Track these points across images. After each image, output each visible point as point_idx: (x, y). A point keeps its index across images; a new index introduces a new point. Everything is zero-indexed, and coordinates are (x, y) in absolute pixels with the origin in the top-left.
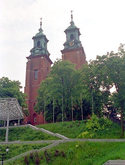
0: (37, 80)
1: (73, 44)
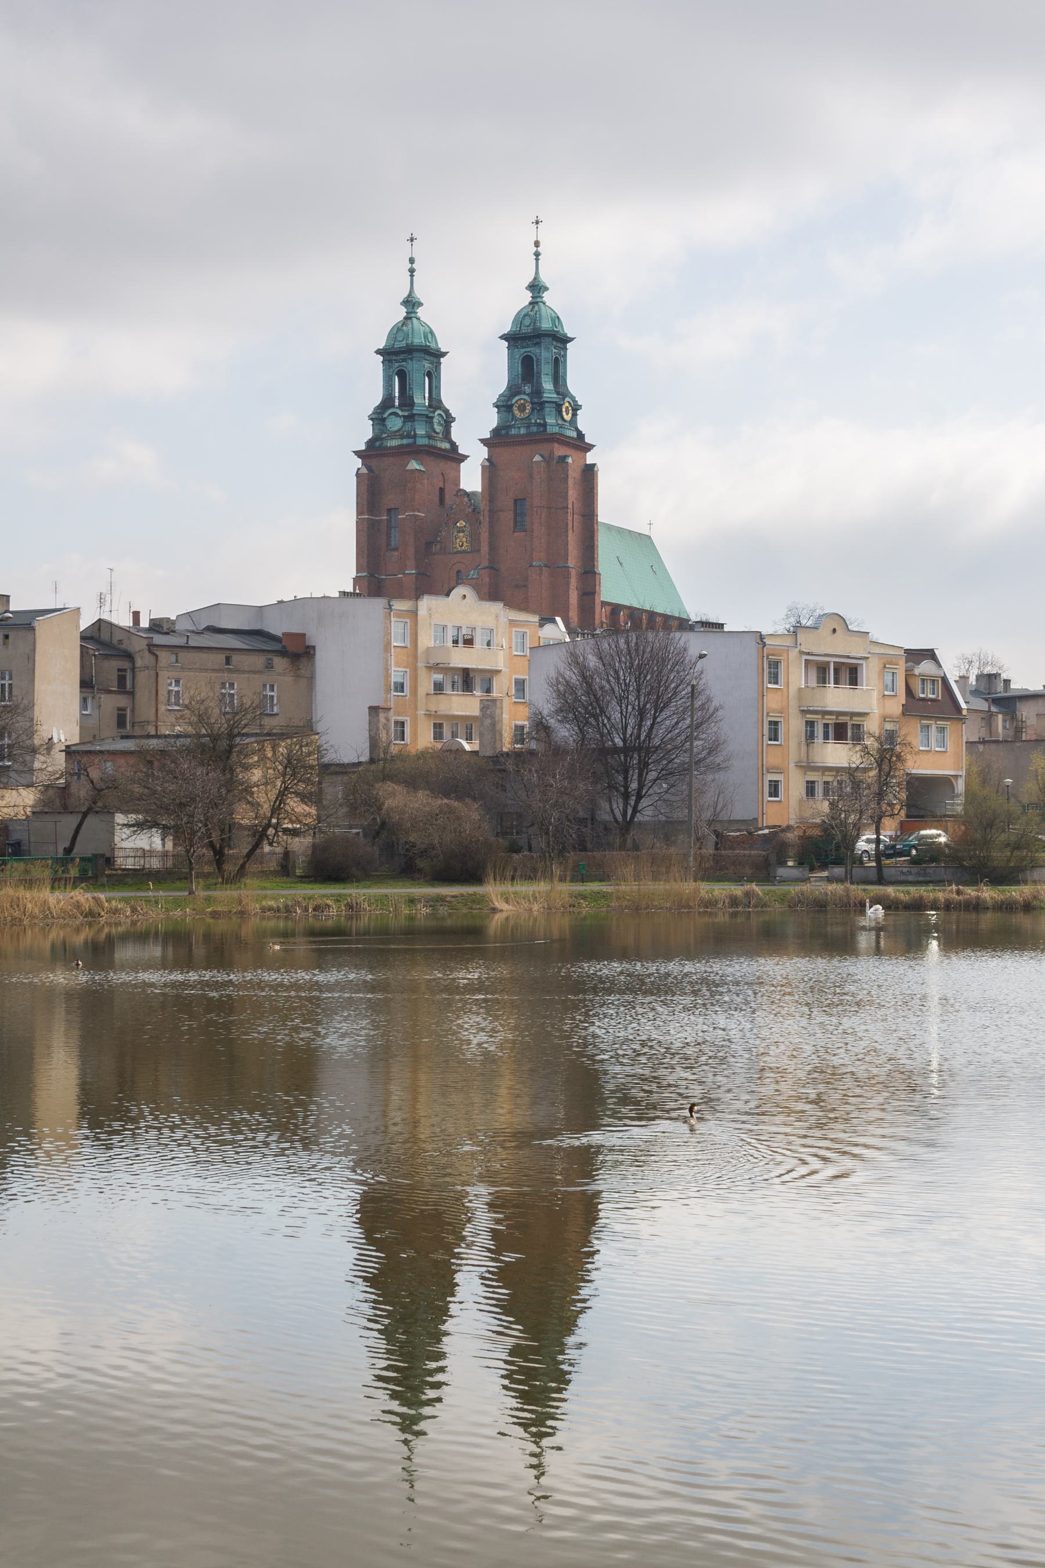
0: (396, 553)
1: (529, 407)
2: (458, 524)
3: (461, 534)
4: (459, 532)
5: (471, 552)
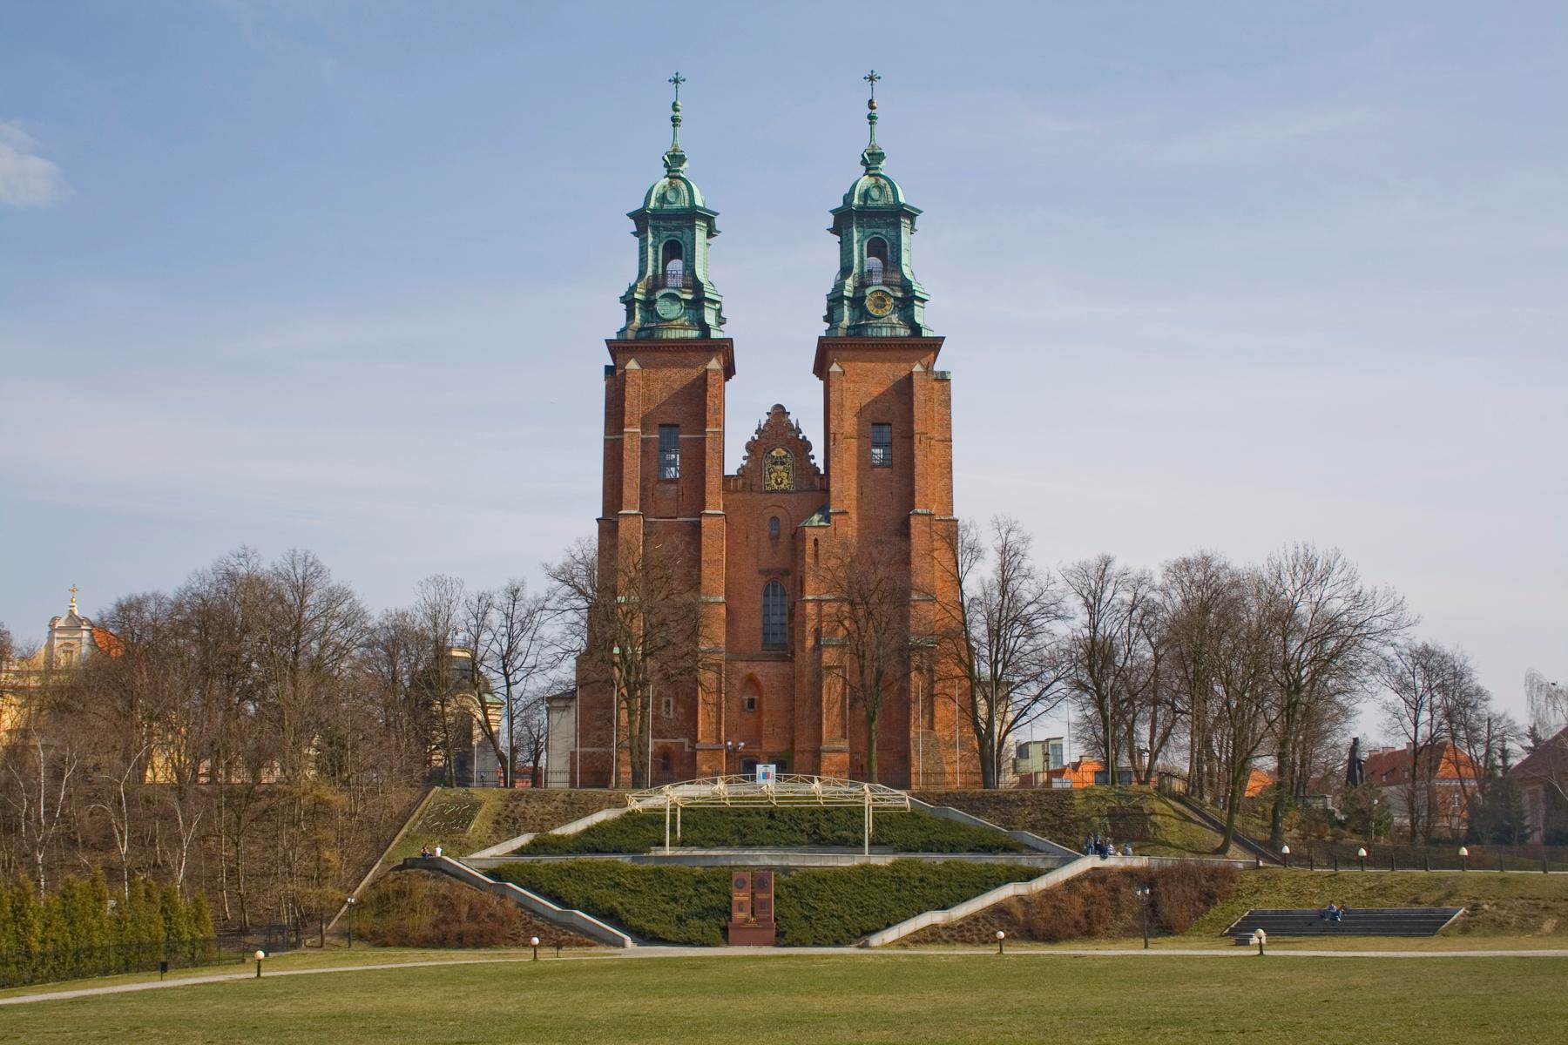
0: (673, 487)
2: (774, 453)
3: (780, 467)
4: (776, 463)
5: (797, 491)
